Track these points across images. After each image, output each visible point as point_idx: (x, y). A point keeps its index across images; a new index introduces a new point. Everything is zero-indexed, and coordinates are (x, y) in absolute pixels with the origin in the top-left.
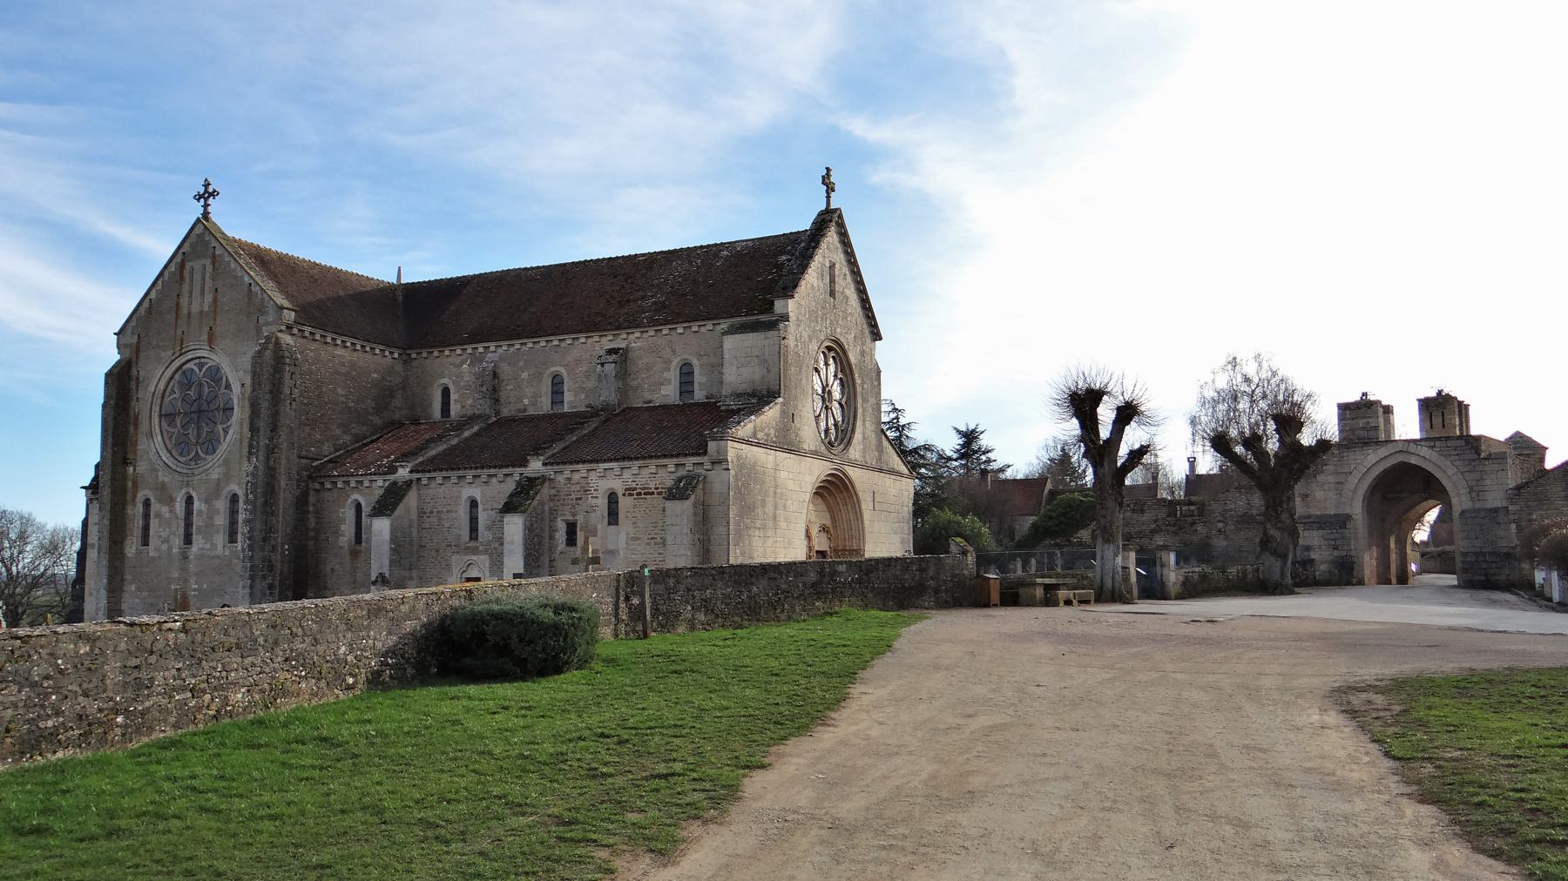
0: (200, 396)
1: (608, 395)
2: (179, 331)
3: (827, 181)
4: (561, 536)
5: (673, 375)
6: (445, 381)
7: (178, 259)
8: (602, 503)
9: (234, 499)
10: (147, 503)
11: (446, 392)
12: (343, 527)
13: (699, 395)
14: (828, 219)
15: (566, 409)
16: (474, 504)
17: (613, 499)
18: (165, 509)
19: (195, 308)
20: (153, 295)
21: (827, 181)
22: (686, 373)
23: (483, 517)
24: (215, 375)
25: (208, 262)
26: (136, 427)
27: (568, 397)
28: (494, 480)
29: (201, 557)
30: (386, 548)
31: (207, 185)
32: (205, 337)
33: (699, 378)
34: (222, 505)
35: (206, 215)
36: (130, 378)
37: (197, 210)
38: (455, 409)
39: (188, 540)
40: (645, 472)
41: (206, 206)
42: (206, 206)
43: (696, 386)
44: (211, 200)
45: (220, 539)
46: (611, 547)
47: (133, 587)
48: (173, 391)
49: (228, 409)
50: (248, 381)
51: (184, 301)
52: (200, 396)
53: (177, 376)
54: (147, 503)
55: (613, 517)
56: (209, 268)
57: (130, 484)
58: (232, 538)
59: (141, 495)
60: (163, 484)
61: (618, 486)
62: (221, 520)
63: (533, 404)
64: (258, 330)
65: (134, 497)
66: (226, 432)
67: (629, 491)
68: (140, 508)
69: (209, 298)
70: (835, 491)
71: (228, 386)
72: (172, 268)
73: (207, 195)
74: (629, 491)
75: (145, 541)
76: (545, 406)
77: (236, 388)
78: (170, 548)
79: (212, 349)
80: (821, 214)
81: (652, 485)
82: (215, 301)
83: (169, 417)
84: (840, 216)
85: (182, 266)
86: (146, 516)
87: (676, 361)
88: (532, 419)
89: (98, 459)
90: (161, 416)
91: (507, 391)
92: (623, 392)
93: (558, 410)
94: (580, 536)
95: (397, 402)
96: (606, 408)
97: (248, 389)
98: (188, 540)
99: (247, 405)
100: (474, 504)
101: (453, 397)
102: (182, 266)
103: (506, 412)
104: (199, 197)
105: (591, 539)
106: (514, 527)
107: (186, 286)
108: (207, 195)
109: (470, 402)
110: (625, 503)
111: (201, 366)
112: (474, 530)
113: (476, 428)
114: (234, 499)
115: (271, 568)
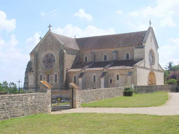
0: (49, 59)
1: (114, 58)
3: (150, 22)
4: (109, 81)
5: (125, 55)
6: (86, 56)
7: (46, 37)
8: (116, 76)
9: (56, 75)
10: (41, 75)
11: (86, 58)
13: (130, 59)
14: (150, 29)
15: (107, 61)
16: (95, 76)
17: (118, 76)
19: (49, 44)
20: (41, 42)
21: (150, 22)
22: (128, 55)
23: (96, 78)
24: (52, 55)
25: (51, 37)
26: (39, 63)
27: (107, 58)
28: (98, 73)
30: (81, 83)
31: (50, 25)
32: (50, 49)
33: (130, 56)
35: (50, 30)
36: (38, 56)
38: (88, 60)
40: (123, 72)
42: (50, 28)
43: (129, 57)
44: (51, 27)
45: (54, 81)
46: (118, 83)
49: (54, 61)
50: (58, 56)
52: (49, 59)
54: (41, 75)
55: (118, 79)
57: (38, 72)
58: (56, 81)
59: (40, 74)
61: (119, 74)
62: (54, 78)
63: (101, 60)
65: (39, 74)
67: (121, 74)
68: (40, 76)
69: (51, 43)
70: (152, 74)
71: (54, 57)
72: (45, 38)
73: (50, 26)
74: (121, 74)
76: (103, 60)
77: (56, 58)
79: (51, 51)
80: (149, 28)
81: (124, 74)
83: (44, 62)
84: (152, 28)
85: (46, 38)
86: (41, 77)
87: (126, 54)
88: (101, 62)
89: (26, 68)
90: (43, 62)
91: (97, 57)
92: (117, 58)
93: (105, 61)
94: (112, 81)
95: (78, 59)
96: (114, 61)
97: (58, 58)
99: (58, 60)
100: (95, 76)
101: (87, 58)
103: (97, 61)
105: (114, 82)
106: (102, 80)
107: (47, 41)
108: (50, 26)
110: (120, 77)
111: (49, 54)
112: (95, 81)
113: (92, 64)
114: (56, 75)
115: (63, 86)
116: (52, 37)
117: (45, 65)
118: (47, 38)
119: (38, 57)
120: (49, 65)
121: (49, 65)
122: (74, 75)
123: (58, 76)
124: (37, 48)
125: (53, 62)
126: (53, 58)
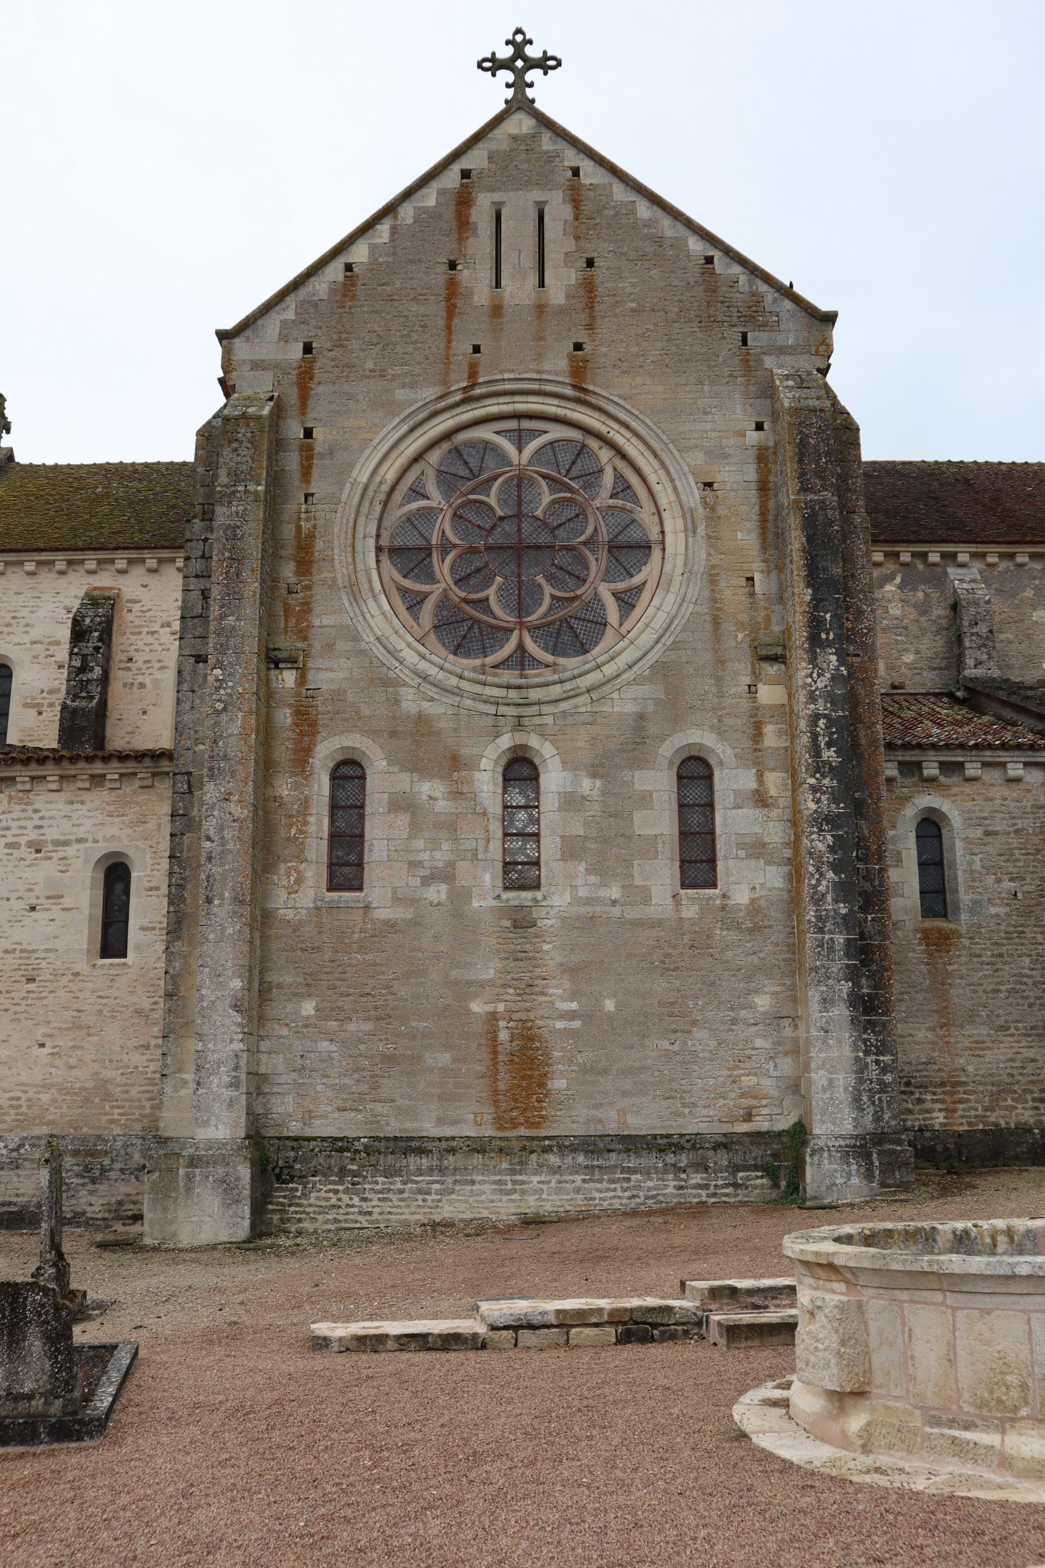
2: (462, 347)
7: (451, 179)
10: (349, 773)
12: (894, 875)
18: (431, 790)
20: (360, 254)
29: (584, 923)
34: (658, 783)
37: (494, 94)
39: (520, 874)
41: (520, 85)
42: (520, 85)
45: (661, 875)
47: (308, 1008)
48: (417, 492)
49: (630, 550)
51: (476, 277)
53: (434, 457)
56: (559, 212)
59: (326, 752)
60: (421, 718)
64: (749, 364)
66: (627, 602)
68: (321, 786)
69: (562, 280)
73: (519, 60)
75: (346, 867)
78: (460, 897)
82: (589, 288)
83: (409, 556)
85: (463, 200)
90: (379, 549)
98: (520, 874)
102: (463, 200)
104: (492, 65)
107: (482, 242)
109: (909, 658)
116: (576, 196)
117: (414, 603)
118: (483, 203)
119: (292, 461)
120: (521, 610)
121: (521, 610)
122: (927, 800)
123: (731, 781)
124: (273, 323)
125: (596, 564)
126: (603, 499)
